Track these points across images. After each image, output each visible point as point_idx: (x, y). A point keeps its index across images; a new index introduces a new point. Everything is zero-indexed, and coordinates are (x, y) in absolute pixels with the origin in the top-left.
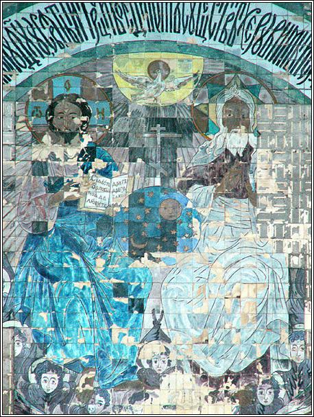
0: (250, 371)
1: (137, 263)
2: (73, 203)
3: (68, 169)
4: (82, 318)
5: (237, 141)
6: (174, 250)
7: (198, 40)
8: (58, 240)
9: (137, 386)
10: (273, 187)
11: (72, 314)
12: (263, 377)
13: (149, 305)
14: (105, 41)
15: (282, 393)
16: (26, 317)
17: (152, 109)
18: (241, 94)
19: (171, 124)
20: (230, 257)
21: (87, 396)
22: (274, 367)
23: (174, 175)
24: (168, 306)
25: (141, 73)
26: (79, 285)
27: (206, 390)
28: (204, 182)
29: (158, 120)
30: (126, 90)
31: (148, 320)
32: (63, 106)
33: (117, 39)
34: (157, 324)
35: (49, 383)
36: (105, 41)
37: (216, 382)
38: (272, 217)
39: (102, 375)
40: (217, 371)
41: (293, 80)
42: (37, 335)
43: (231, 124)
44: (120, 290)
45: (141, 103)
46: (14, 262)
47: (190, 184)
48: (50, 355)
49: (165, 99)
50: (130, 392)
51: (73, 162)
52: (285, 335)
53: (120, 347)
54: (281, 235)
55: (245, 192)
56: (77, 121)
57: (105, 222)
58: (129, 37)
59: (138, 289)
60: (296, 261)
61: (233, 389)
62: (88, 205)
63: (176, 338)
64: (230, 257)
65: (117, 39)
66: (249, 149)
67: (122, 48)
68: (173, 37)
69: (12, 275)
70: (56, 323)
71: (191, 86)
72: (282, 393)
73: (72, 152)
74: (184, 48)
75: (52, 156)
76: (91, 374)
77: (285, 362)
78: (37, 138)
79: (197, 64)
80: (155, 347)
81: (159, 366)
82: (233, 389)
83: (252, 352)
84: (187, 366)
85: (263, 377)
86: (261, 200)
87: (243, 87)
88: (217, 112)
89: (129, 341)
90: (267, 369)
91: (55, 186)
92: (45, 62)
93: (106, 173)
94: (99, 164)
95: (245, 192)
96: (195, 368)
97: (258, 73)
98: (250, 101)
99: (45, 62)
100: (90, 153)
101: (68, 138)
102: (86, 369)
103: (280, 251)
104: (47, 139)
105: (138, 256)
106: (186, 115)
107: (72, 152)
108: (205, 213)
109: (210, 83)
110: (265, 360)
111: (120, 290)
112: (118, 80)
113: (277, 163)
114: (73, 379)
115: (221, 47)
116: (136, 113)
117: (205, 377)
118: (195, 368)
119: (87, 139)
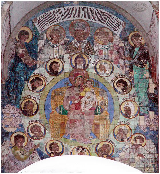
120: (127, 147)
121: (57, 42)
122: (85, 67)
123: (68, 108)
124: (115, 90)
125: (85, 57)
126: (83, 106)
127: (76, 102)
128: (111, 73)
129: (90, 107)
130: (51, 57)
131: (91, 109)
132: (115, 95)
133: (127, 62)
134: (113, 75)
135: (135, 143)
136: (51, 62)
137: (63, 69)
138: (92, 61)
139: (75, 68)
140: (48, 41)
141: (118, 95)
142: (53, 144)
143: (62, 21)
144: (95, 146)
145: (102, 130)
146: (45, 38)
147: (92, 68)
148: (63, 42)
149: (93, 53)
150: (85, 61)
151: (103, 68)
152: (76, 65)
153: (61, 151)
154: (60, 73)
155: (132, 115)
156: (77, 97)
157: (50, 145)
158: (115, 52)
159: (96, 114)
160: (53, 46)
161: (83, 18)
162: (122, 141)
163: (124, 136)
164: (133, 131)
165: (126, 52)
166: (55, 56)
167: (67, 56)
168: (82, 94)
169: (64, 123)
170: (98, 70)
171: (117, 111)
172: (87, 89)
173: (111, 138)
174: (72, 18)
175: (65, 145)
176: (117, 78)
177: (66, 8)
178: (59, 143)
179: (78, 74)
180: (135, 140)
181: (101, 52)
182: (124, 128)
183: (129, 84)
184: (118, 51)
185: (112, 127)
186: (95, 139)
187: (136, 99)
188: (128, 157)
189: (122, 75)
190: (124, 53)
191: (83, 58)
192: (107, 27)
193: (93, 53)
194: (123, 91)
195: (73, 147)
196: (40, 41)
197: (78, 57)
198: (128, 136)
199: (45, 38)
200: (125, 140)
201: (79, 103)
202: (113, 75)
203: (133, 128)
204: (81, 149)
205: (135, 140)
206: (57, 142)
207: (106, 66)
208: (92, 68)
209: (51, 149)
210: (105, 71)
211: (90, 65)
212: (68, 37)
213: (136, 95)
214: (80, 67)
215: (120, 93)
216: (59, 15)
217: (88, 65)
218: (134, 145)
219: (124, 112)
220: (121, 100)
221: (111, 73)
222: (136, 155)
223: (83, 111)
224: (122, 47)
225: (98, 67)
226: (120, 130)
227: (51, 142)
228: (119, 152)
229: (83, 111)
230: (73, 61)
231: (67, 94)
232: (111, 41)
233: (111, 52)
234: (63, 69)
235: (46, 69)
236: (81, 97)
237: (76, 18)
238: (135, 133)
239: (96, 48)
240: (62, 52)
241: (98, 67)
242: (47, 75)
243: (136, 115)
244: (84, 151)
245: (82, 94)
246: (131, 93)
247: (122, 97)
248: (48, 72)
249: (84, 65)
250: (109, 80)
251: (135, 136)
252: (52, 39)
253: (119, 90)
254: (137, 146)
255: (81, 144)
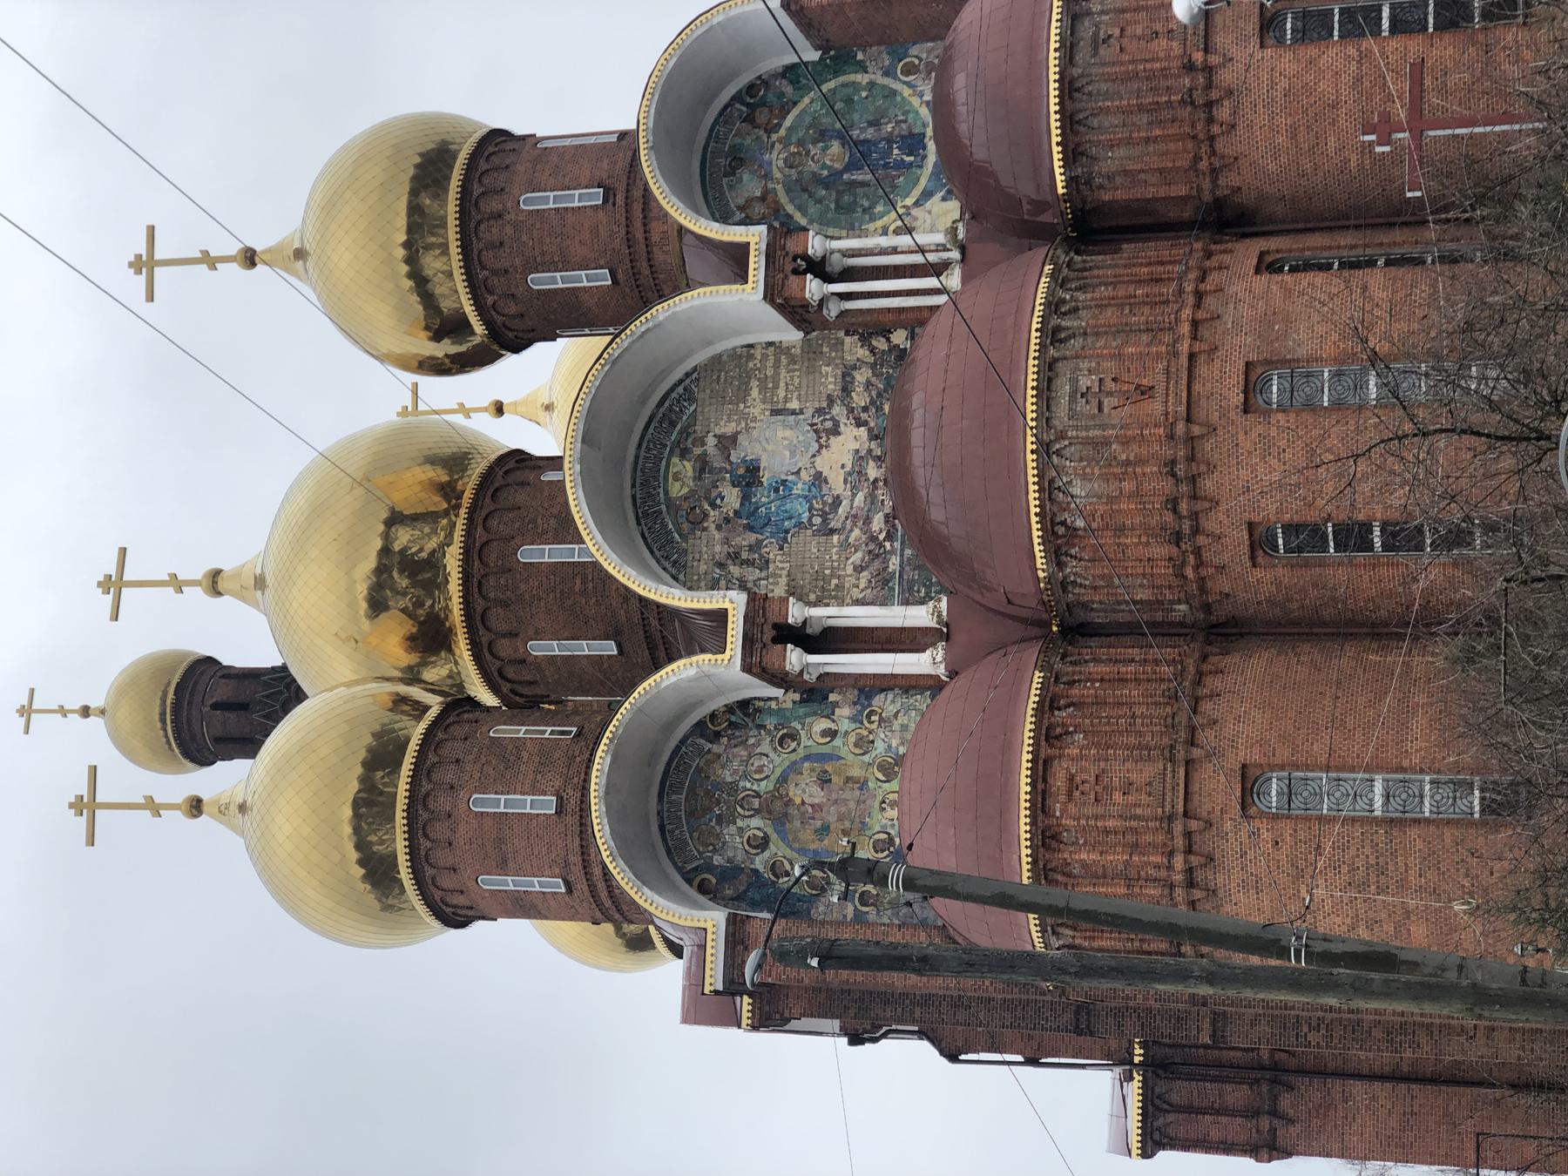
0: (816, 431)
1: (765, 484)
2: (736, 512)
3: (720, 515)
4: (788, 507)
5: (711, 441)
6: (759, 468)
7: (665, 460)
8: (752, 518)
9: (821, 482)
10: (734, 424)
11: (786, 511)
12: (819, 426)
13: (784, 477)
14: (662, 500)
15: (827, 417)
16: (787, 532)
17: (694, 479)
18: (690, 440)
19: (702, 470)
20: (764, 443)
21: (824, 503)
22: (815, 421)
23: (725, 468)
24: (785, 469)
25: (677, 485)
26: (773, 509)
27: (824, 451)
28: (729, 455)
29: (700, 476)
30: (685, 490)
31: (790, 478)
32: (691, 518)
33: (662, 495)
34: (793, 474)
35: (817, 520)
36: (662, 500)
37: (821, 447)
38: (747, 424)
39: (816, 498)
40: (816, 446)
41: (685, 418)
42: (795, 526)
43: (703, 444)
44: (777, 490)
45: (691, 484)
46: (761, 537)
47: (730, 461)
48: (805, 520)
49: (690, 473)
50: (823, 485)
51: (717, 513)
52: (802, 417)
53: (802, 490)
54: (755, 420)
55: (734, 438)
56: (698, 511)
57: (745, 498)
58: (661, 490)
59: (776, 482)
60: (767, 413)
61: (824, 439)
62: (737, 506)
63: (800, 465)
64: (764, 443)
65: (662, 495)
66: (715, 436)
67: (666, 492)
68: (662, 471)
69: (767, 538)
70: (790, 518)
71: (685, 463)
72: (827, 417)
73: (712, 513)
74: (668, 466)
75: (713, 522)
76: (814, 502)
77: (813, 416)
78: (705, 529)
79: (675, 460)
80: (803, 474)
81: (812, 472)
82: (824, 439)
83: (808, 431)
84: (812, 460)
85: (819, 426)
86: (739, 429)
87: (686, 440)
88: (698, 451)
89: (800, 486)
90: (816, 424)
91: (727, 520)
92: (671, 526)
93: (723, 498)
94: (718, 501)
95: (734, 438)
96: (814, 456)
97: (680, 433)
98: (693, 436)
99: (671, 526)
100: (713, 505)
101: (706, 515)
102: (812, 504)
103: (761, 421)
104: (705, 525)
105: (762, 482)
106: (698, 465)
107: (712, 513)
108: (743, 454)
109: (684, 454)
110: (812, 425)
111: (777, 490)
112: (680, 494)
113: (722, 423)
114: (816, 510)
115: (668, 449)
116: (696, 485)
117: (818, 451)
118: (814, 456)
119: (706, 506)
120: (882, 736)
121: (718, 836)
122: (758, 795)
123: (819, 824)
124: (794, 750)
125: (742, 795)
126: (817, 801)
127: (810, 810)
128: (767, 756)
129: (819, 790)
130: (740, 846)
131: (822, 790)
132: (801, 752)
133: (751, 733)
134: (772, 755)
135: (876, 723)
136: (747, 847)
137: (759, 829)
138: (748, 785)
139: (757, 812)
140: (715, 851)
141: (802, 746)
142: (874, 847)
143: (685, 829)
144: (879, 784)
145: (856, 772)
146: (710, 854)
147: (759, 785)
148: (717, 828)
149: (735, 783)
150: (748, 796)
151: (760, 770)
152: (753, 809)
153: (886, 836)
154: (765, 833)
155: (833, 726)
156: (802, 808)
157: (877, 852)
158: (736, 750)
159: (830, 780)
160: (724, 843)
161: (683, 796)
162: (873, 742)
163: (866, 739)
164: (859, 725)
165: (737, 734)
166: (738, 840)
167: (740, 823)
168: (798, 801)
169: (843, 830)
170: (763, 776)
171: (826, 750)
172: (791, 794)
173: (866, 758)
174: (683, 813)
175: (877, 828)
176: (775, 749)
177: (666, 822)
178: (877, 837)
179: (768, 806)
180: (873, 722)
181: (736, 772)
182: (852, 739)
183: (785, 731)
184: (735, 746)
185: (850, 757)
186: (870, 784)
187: (808, 720)
188: (898, 734)
189: (772, 741)
190: (737, 737)
191: (743, 799)
192: (697, 761)
193: (735, 783)
194: (795, 739)
195: (880, 817)
196: (716, 863)
197: (742, 807)
198: (865, 733)
199: (710, 854)
200: (871, 737)
201: (812, 806)
202: (772, 755)
203: (853, 726)
204: (883, 805)
205: (873, 722)
206: (872, 841)
207: (756, 765)
208: (759, 785)
209: (882, 851)
210: (764, 765)
211: (755, 787)
212: (711, 820)
213: (802, 721)
214: (756, 803)
215: (799, 744)
216: (677, 832)
217: (754, 791)
218: (880, 724)
219: (828, 739)
220: (810, 743)
221: (767, 756)
222: (895, 722)
223: (824, 800)
224: (729, 740)
225: (757, 777)
226: (856, 745)
227: (872, 850)
228: (890, 747)
229: (824, 800)
230: (747, 813)
231: (797, 824)
232: (719, 756)
233: (734, 756)
234: (759, 829)
235: (757, 854)
236: (803, 803)
237: (683, 808)
238: (862, 723)
239: (729, 779)
240: (732, 829)
241: (757, 777)
242: (766, 854)
243: (834, 721)
244: (887, 801)
245: (798, 801)
246: (799, 727)
247: (805, 741)
248: (763, 852)
249: (754, 797)
250: (777, 760)
251: (865, 722)
252: (711, 844)
253: (794, 745)
254: (881, 720)
255: (877, 804)
